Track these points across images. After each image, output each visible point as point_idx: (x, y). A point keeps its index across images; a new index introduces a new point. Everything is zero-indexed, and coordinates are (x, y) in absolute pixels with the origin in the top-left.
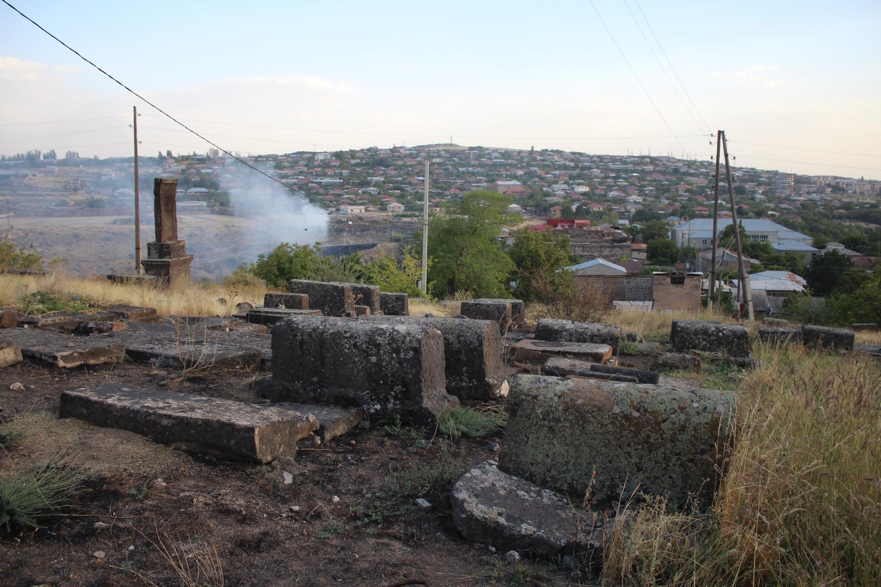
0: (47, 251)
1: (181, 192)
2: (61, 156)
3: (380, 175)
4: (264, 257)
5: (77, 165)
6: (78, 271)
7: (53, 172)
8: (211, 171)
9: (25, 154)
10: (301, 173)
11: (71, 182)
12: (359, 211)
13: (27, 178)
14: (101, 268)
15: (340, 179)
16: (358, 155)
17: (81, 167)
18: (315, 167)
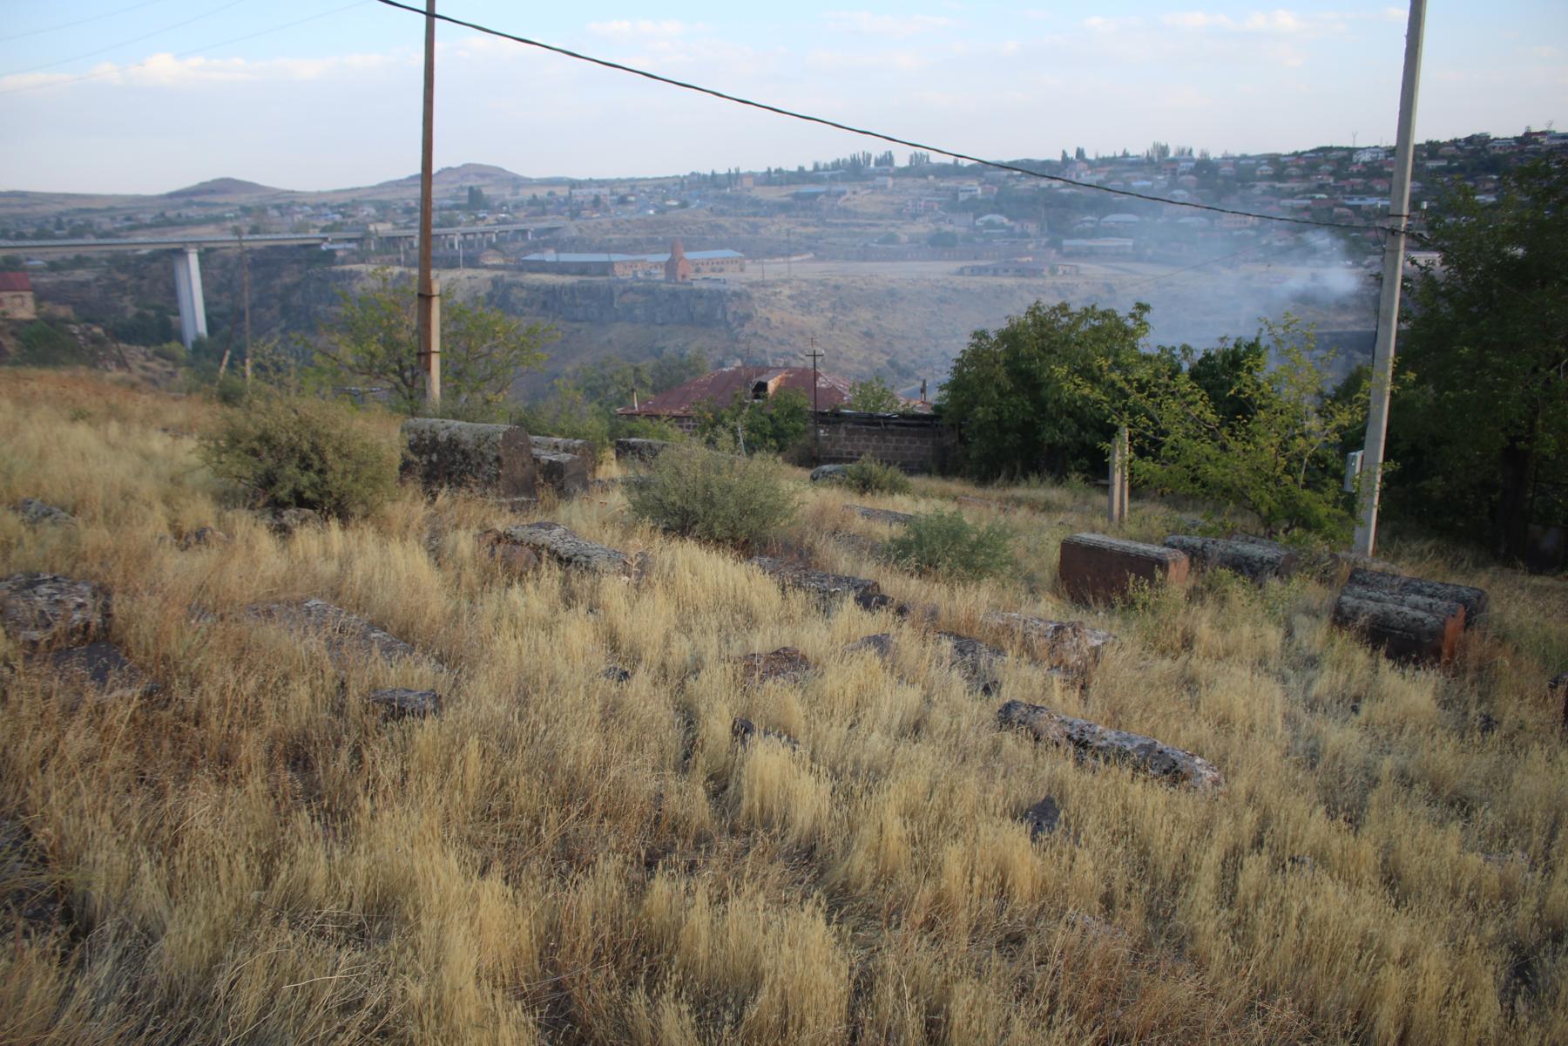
0: (840, 317)
1: (1092, 222)
3: (1487, 192)
4: (987, 338)
5: (924, 175)
6: (887, 354)
7: (884, 187)
8: (1149, 183)
9: (849, 158)
10: (1321, 188)
11: (910, 203)
13: (844, 198)
14: (927, 350)
16: (1442, 151)
18: (1352, 175)
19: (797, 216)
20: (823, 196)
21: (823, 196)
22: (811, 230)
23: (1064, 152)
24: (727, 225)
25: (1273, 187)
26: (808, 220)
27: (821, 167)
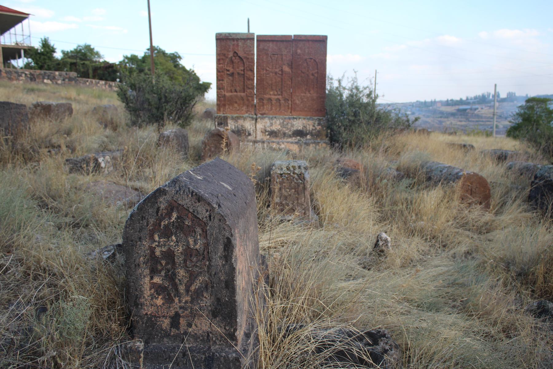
13: (477, 111)
19: (458, 118)
22: (463, 123)
24: (430, 121)
26: (461, 119)
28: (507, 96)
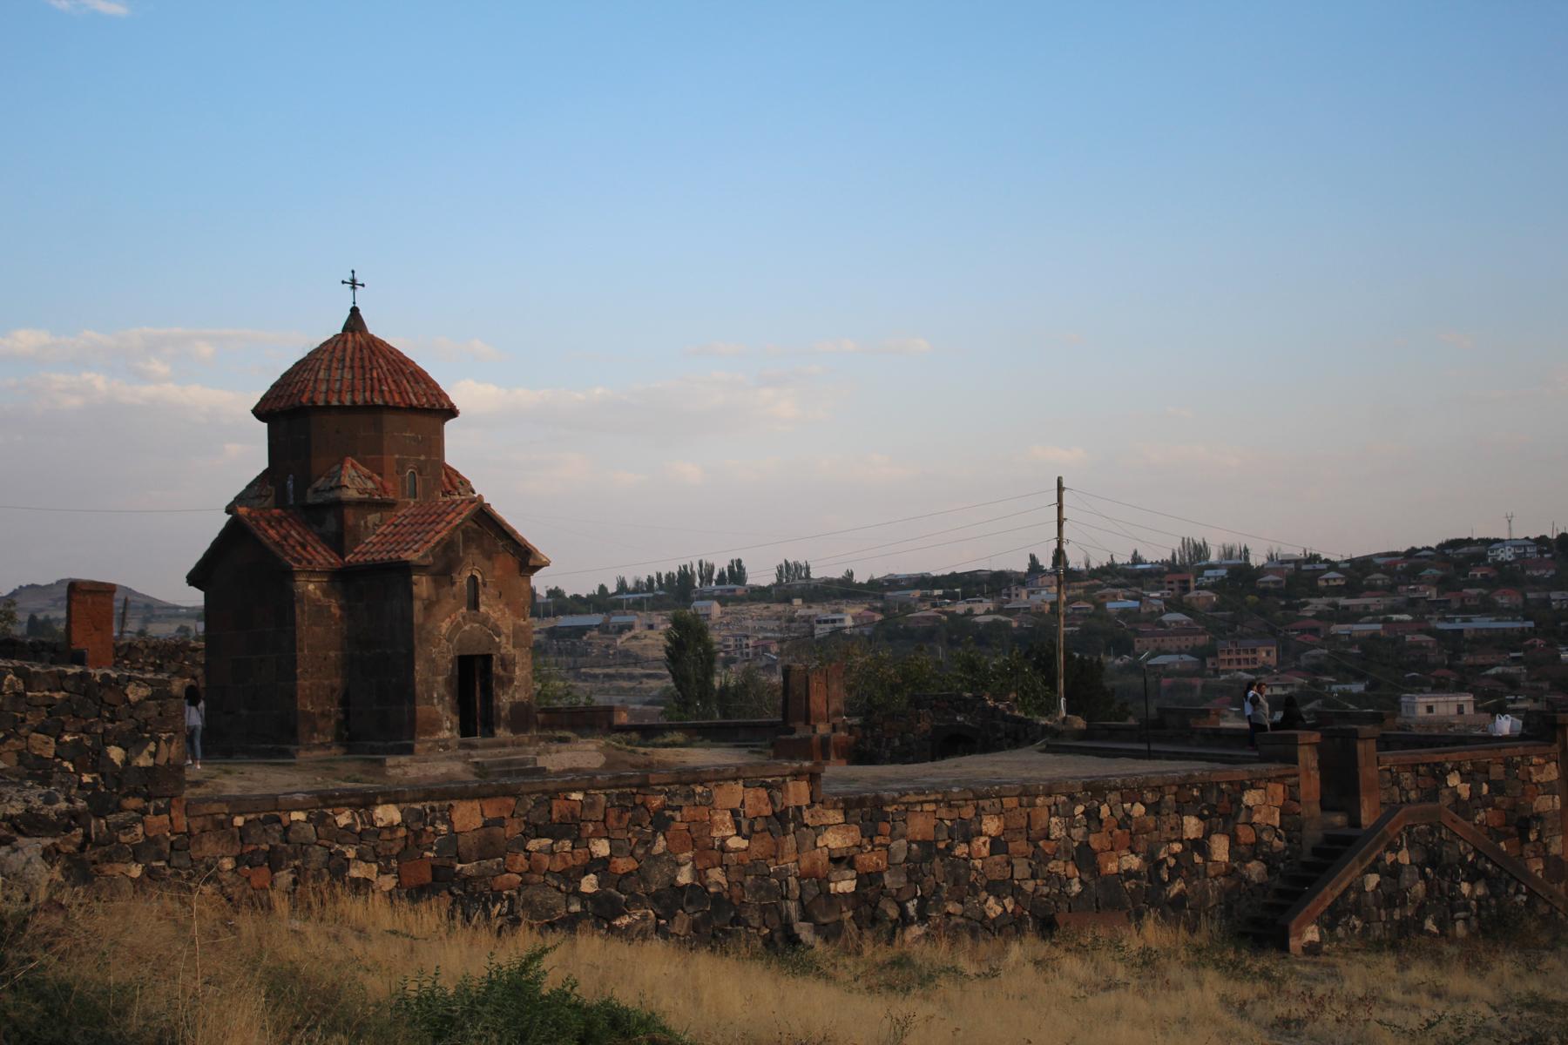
2: (761, 575)
5: (787, 600)
11: (731, 642)
12: (1453, 710)
15: (1527, 619)
17: (797, 602)
20: (595, 633)
21: (595, 633)
23: (1033, 558)
25: (1335, 606)
27: (630, 584)
28: (779, 580)
